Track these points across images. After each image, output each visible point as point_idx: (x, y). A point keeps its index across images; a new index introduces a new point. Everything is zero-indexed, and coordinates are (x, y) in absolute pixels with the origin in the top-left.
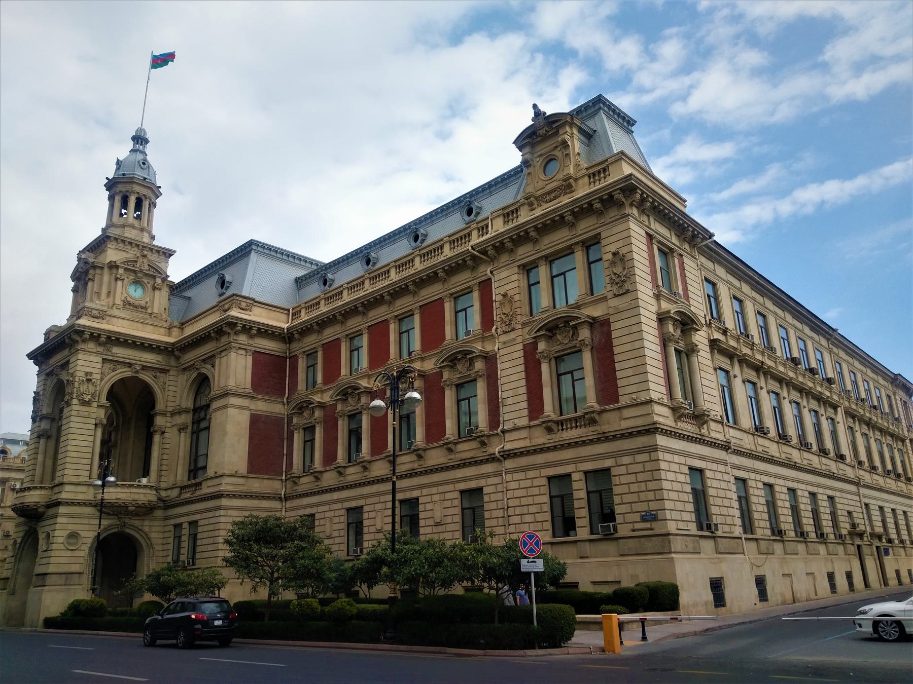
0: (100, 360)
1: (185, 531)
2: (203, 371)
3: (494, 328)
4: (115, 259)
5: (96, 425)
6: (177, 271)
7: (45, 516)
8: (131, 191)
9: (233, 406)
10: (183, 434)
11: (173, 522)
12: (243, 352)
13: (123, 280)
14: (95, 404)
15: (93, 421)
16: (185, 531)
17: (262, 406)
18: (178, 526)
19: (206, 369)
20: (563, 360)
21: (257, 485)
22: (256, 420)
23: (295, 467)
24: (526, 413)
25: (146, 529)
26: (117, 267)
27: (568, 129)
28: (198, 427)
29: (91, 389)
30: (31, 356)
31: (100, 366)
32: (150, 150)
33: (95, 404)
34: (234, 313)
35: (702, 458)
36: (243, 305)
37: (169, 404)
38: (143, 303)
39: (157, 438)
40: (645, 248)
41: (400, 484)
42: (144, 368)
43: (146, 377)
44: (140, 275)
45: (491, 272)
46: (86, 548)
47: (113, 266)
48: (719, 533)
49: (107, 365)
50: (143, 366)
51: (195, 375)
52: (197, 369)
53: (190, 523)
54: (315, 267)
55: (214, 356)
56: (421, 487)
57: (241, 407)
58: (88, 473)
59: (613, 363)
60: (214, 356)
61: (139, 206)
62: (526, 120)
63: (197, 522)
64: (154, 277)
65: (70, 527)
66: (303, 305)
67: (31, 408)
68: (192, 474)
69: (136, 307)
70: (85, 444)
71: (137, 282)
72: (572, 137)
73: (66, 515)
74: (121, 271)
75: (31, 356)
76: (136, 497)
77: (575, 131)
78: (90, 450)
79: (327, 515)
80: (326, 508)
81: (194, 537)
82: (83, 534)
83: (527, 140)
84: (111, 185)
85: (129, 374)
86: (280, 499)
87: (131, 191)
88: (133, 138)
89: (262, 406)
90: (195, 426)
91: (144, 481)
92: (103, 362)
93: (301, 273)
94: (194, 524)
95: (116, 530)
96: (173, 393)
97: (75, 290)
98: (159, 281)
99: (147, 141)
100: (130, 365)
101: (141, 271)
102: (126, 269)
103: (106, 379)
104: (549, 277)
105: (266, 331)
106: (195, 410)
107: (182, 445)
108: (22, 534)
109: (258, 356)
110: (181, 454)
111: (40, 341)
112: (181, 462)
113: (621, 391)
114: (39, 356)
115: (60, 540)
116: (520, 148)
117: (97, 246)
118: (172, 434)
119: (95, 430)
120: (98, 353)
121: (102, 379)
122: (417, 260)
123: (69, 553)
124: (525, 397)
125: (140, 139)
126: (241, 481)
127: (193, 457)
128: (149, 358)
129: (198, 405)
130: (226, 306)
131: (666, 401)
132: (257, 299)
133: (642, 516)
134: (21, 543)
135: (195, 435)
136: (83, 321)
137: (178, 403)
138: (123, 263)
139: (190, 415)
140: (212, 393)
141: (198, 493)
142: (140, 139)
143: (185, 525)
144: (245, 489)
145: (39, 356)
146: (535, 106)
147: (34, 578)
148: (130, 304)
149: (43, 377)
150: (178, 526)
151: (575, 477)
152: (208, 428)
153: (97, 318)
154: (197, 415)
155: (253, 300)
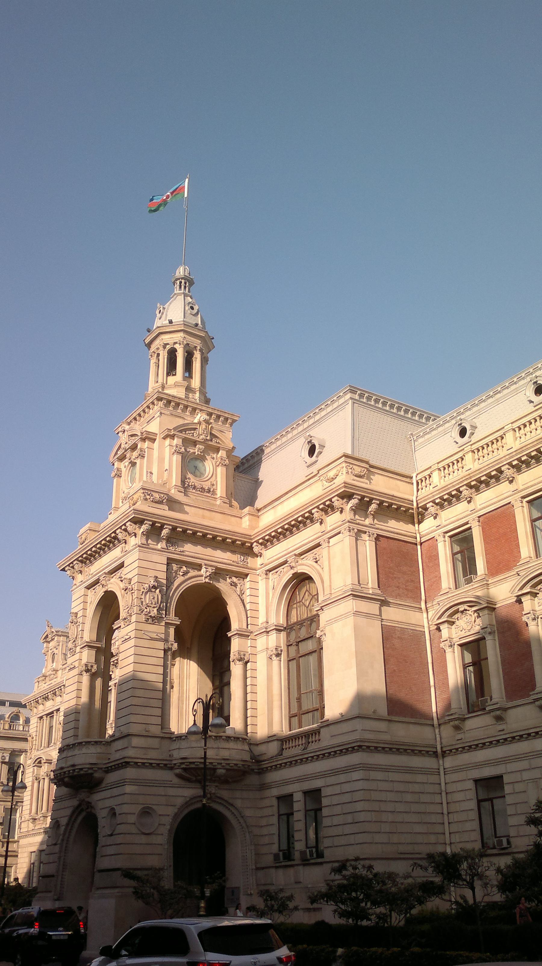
1: (299, 805)
2: (300, 569)
7: (103, 785)
11: (275, 792)
16: (299, 805)
19: (305, 566)
25: (238, 803)
28: (298, 651)
31: (164, 568)
39: (236, 669)
46: (165, 830)
50: (217, 568)
51: (289, 575)
52: (292, 568)
53: (306, 793)
55: (318, 545)
60: (318, 545)
66: (436, 467)
68: (295, 720)
79: (526, 775)
80: (524, 764)
82: (161, 810)
86: (435, 754)
90: (293, 649)
92: (168, 564)
94: (314, 795)
106: (288, 629)
107: (276, 678)
108: (68, 812)
118: (261, 663)
122: (469, 457)
123: (143, 839)
126: (382, 726)
127: (295, 695)
129: (294, 619)
130: (331, 474)
134: (67, 824)
135: (293, 664)
139: (283, 635)
140: (321, 598)
141: (313, 747)
143: (298, 797)
147: (97, 876)
152: (319, 651)
154: (293, 635)
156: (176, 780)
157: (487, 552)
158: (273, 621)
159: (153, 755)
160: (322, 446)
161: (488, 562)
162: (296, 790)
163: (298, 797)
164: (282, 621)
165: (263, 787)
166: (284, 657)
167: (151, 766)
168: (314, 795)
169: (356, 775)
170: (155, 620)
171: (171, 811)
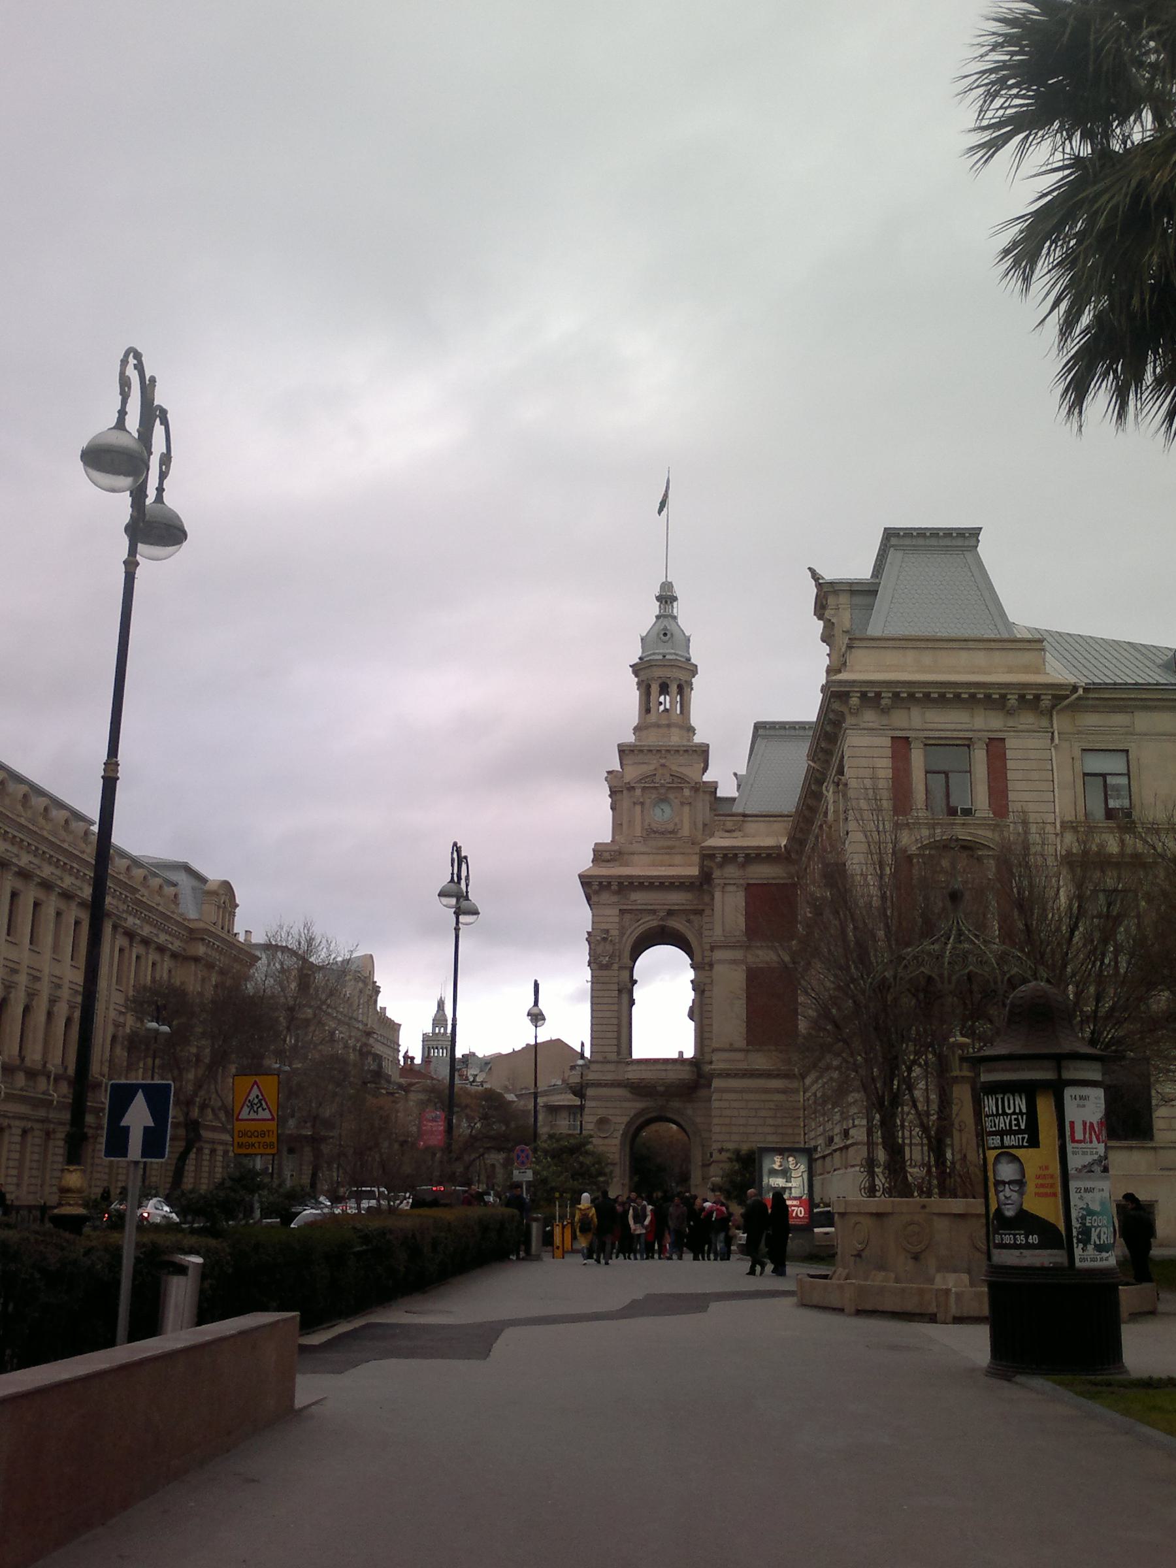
4: (655, 768)
5: (620, 991)
8: (664, 674)
9: (720, 961)
13: (642, 804)
14: (616, 966)
15: (616, 987)
17: (765, 956)
21: (760, 1061)
22: (754, 976)
25: (689, 1112)
29: (609, 948)
31: (617, 919)
32: (679, 609)
33: (616, 966)
36: (729, 825)
38: (670, 827)
42: (670, 913)
43: (676, 924)
44: (663, 791)
46: (618, 1134)
49: (627, 916)
57: (734, 962)
58: (615, 1049)
64: (682, 788)
65: (600, 1111)
69: (662, 833)
71: (664, 800)
73: (594, 1098)
74: (638, 792)
76: (663, 1075)
85: (655, 923)
87: (664, 674)
88: (659, 599)
89: (765, 956)
98: (687, 792)
99: (675, 599)
100: (654, 912)
101: (662, 786)
102: (644, 788)
105: (758, 855)
109: (751, 890)
119: (619, 997)
120: (614, 904)
121: (622, 934)
125: (666, 598)
126: (740, 1056)
128: (676, 898)
138: (640, 781)
142: (666, 598)
144: (743, 1066)
148: (655, 832)
153: (608, 861)
155: (745, 815)
156: (629, 1095)
159: (609, 1077)
167: (606, 1085)
170: (606, 967)
171: (625, 1120)
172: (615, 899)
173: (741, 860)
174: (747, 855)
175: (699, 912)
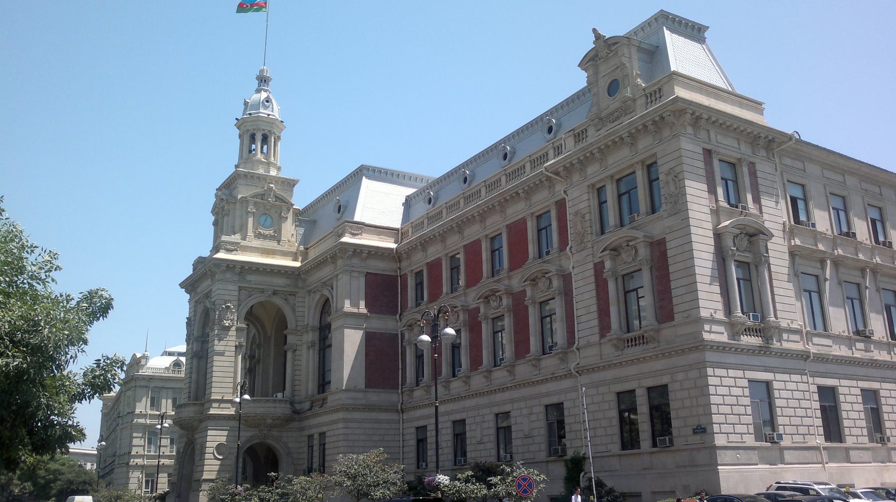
0: (237, 288)
3: (568, 248)
6: (301, 199)
10: (311, 351)
12: (356, 274)
16: (316, 442)
18: (310, 437)
20: (632, 277)
23: (408, 381)
24: (597, 330)
26: (247, 201)
27: (626, 50)
28: (324, 344)
30: (182, 285)
31: (236, 293)
34: (347, 239)
35: (767, 369)
37: (299, 323)
39: (289, 355)
40: (701, 165)
41: (442, 409)
42: (275, 293)
43: (278, 301)
45: (565, 192)
47: (244, 201)
48: (783, 444)
54: (424, 184)
56: (512, 401)
59: (669, 281)
61: (265, 139)
62: (589, 44)
63: (324, 433)
67: (184, 332)
70: (228, 364)
72: (630, 58)
75: (182, 285)
77: (634, 51)
78: (232, 370)
81: (323, 445)
83: (590, 62)
84: (240, 124)
86: (397, 411)
91: (280, 395)
92: (240, 290)
93: (410, 191)
94: (322, 435)
95: (258, 441)
96: (303, 314)
97: (216, 224)
103: (243, 305)
104: (616, 195)
110: (311, 370)
111: (189, 271)
112: (311, 377)
113: (676, 309)
114: (189, 285)
115: (211, 450)
116: (586, 70)
117: (229, 186)
124: (595, 315)
126: (361, 395)
130: (340, 232)
131: (720, 316)
132: (367, 222)
133: (694, 430)
136: (221, 255)
137: (306, 322)
138: (253, 197)
145: (189, 285)
146: (594, 30)
149: (193, 304)
150: (310, 437)
151: (639, 392)
157: (429, 287)
158: (311, 323)
160: (346, 207)
161: (430, 294)
162: (315, 432)
163: (316, 436)
164: (317, 324)
165: (302, 429)
166: (317, 347)
168: (322, 435)
169: (341, 425)
172: (236, 278)
173: (364, 255)
174: (369, 252)
175: (293, 294)
